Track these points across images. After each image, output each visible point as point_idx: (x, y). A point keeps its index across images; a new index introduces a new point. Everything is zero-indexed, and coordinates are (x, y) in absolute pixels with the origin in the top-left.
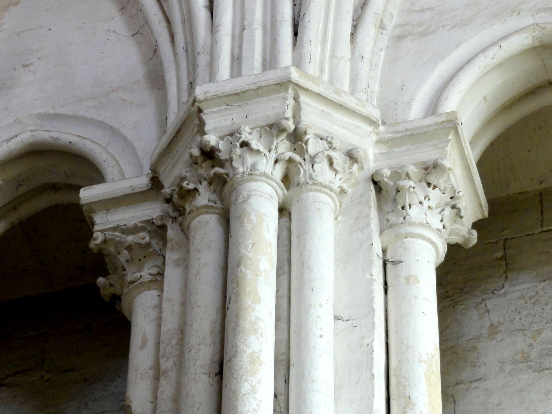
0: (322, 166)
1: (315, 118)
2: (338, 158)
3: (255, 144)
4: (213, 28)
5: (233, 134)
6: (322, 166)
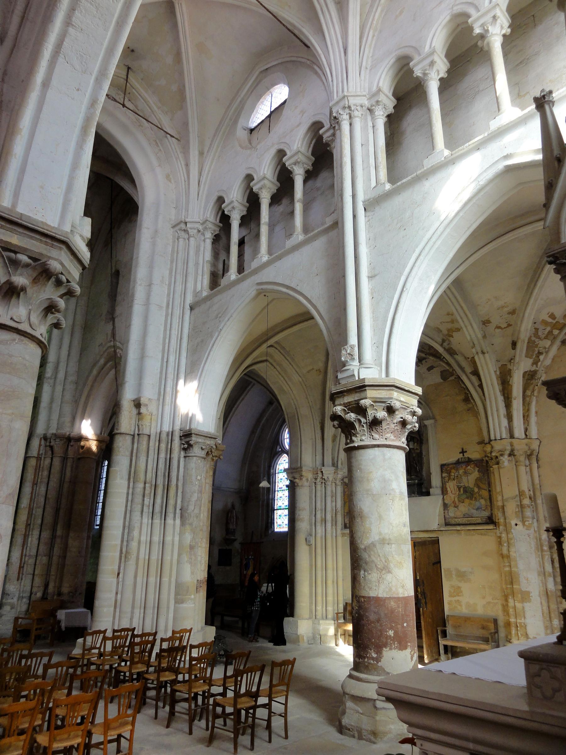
1: (352, 101)
2: (359, 108)
4: (333, 85)
5: (338, 112)
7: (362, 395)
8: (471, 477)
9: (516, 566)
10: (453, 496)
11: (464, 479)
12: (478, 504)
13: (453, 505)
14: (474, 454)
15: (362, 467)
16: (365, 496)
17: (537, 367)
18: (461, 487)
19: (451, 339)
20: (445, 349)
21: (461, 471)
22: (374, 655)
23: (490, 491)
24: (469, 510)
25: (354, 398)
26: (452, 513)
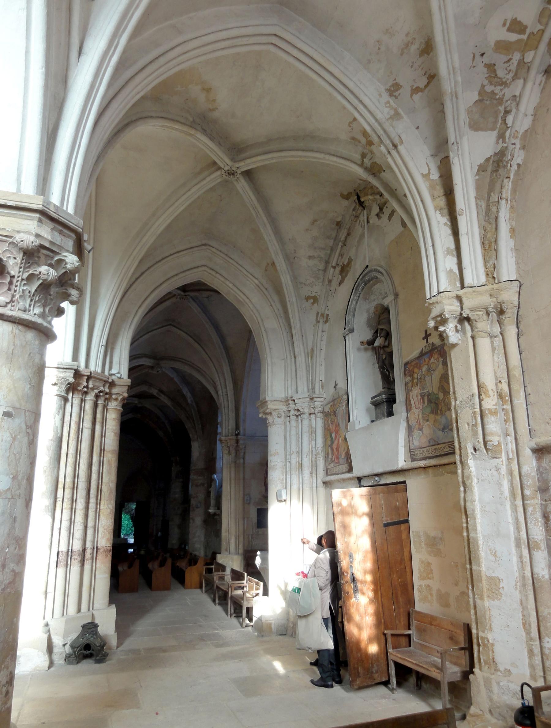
17: (504, 141)
20: (366, 169)
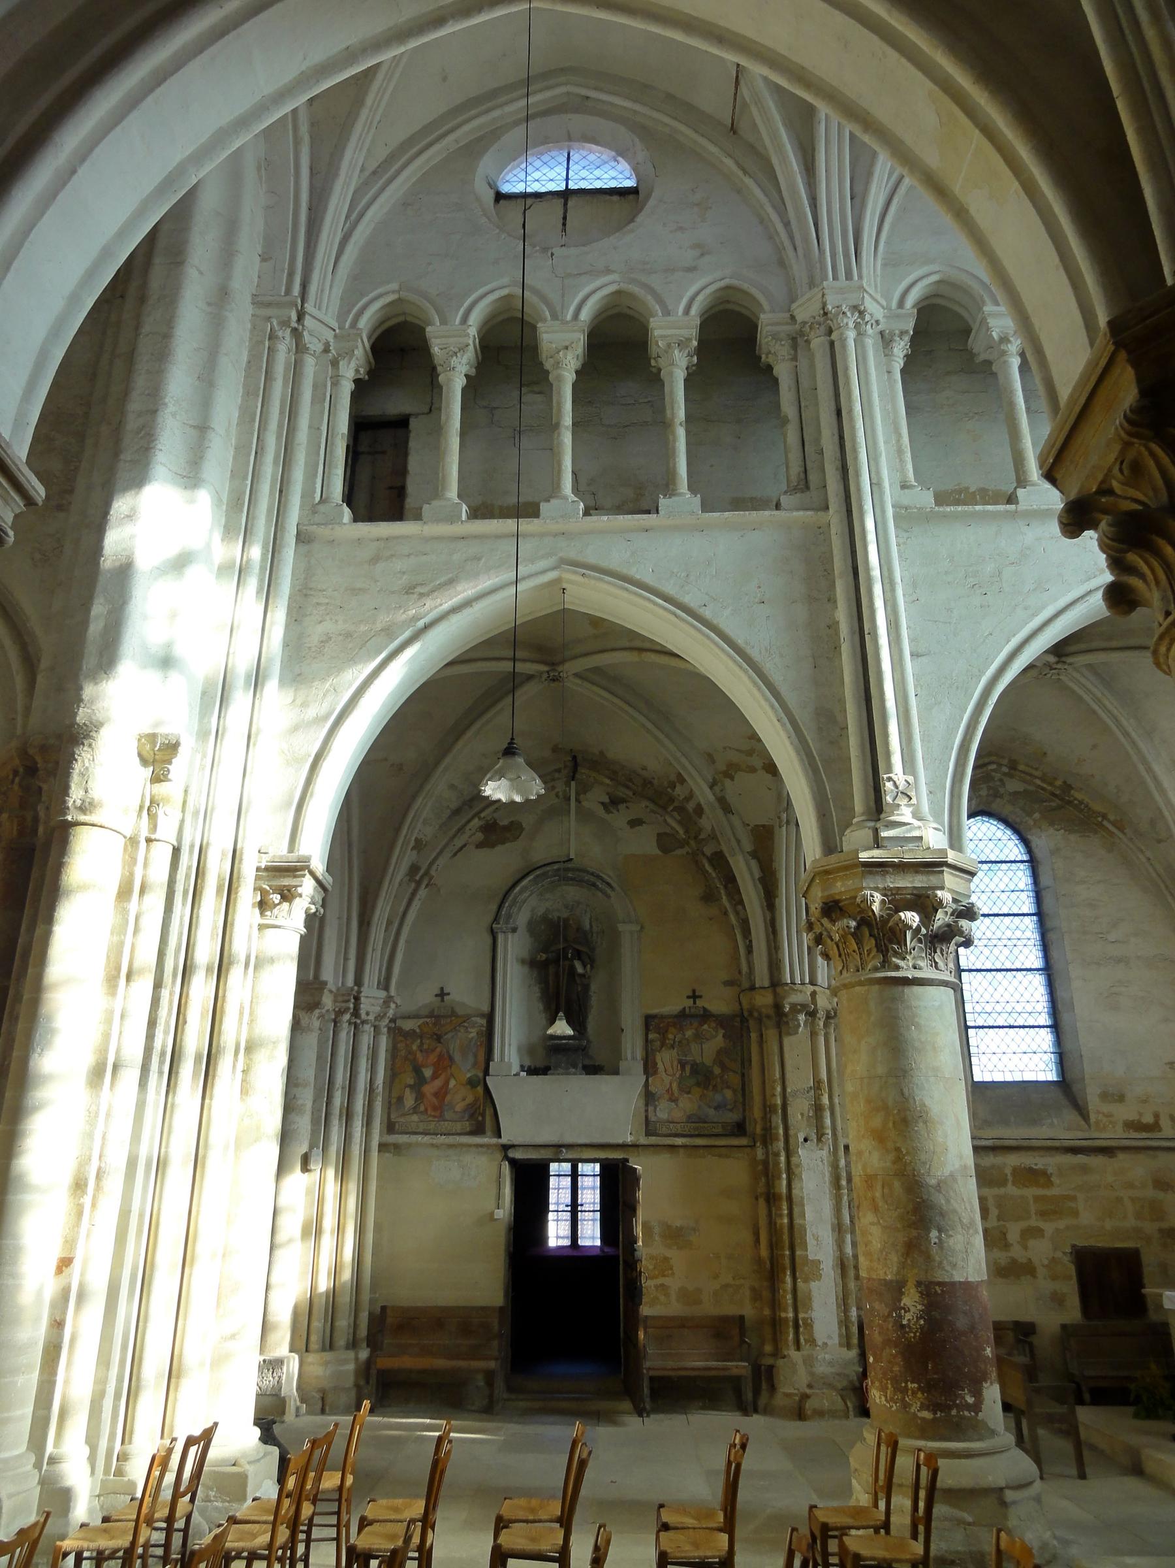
0: (869, 326)
1: (870, 305)
3: (849, 314)
6: (869, 326)
7: (933, 880)
8: (710, 1046)
9: (803, 1215)
10: (667, 1080)
11: (694, 1047)
12: (718, 1097)
13: (667, 1097)
14: (718, 1002)
15: (922, 1022)
16: (932, 1079)
18: (687, 1062)
19: (728, 782)
21: (689, 1033)
22: (970, 1400)
23: (743, 1075)
24: (699, 1107)
25: (912, 882)
26: (663, 1111)
